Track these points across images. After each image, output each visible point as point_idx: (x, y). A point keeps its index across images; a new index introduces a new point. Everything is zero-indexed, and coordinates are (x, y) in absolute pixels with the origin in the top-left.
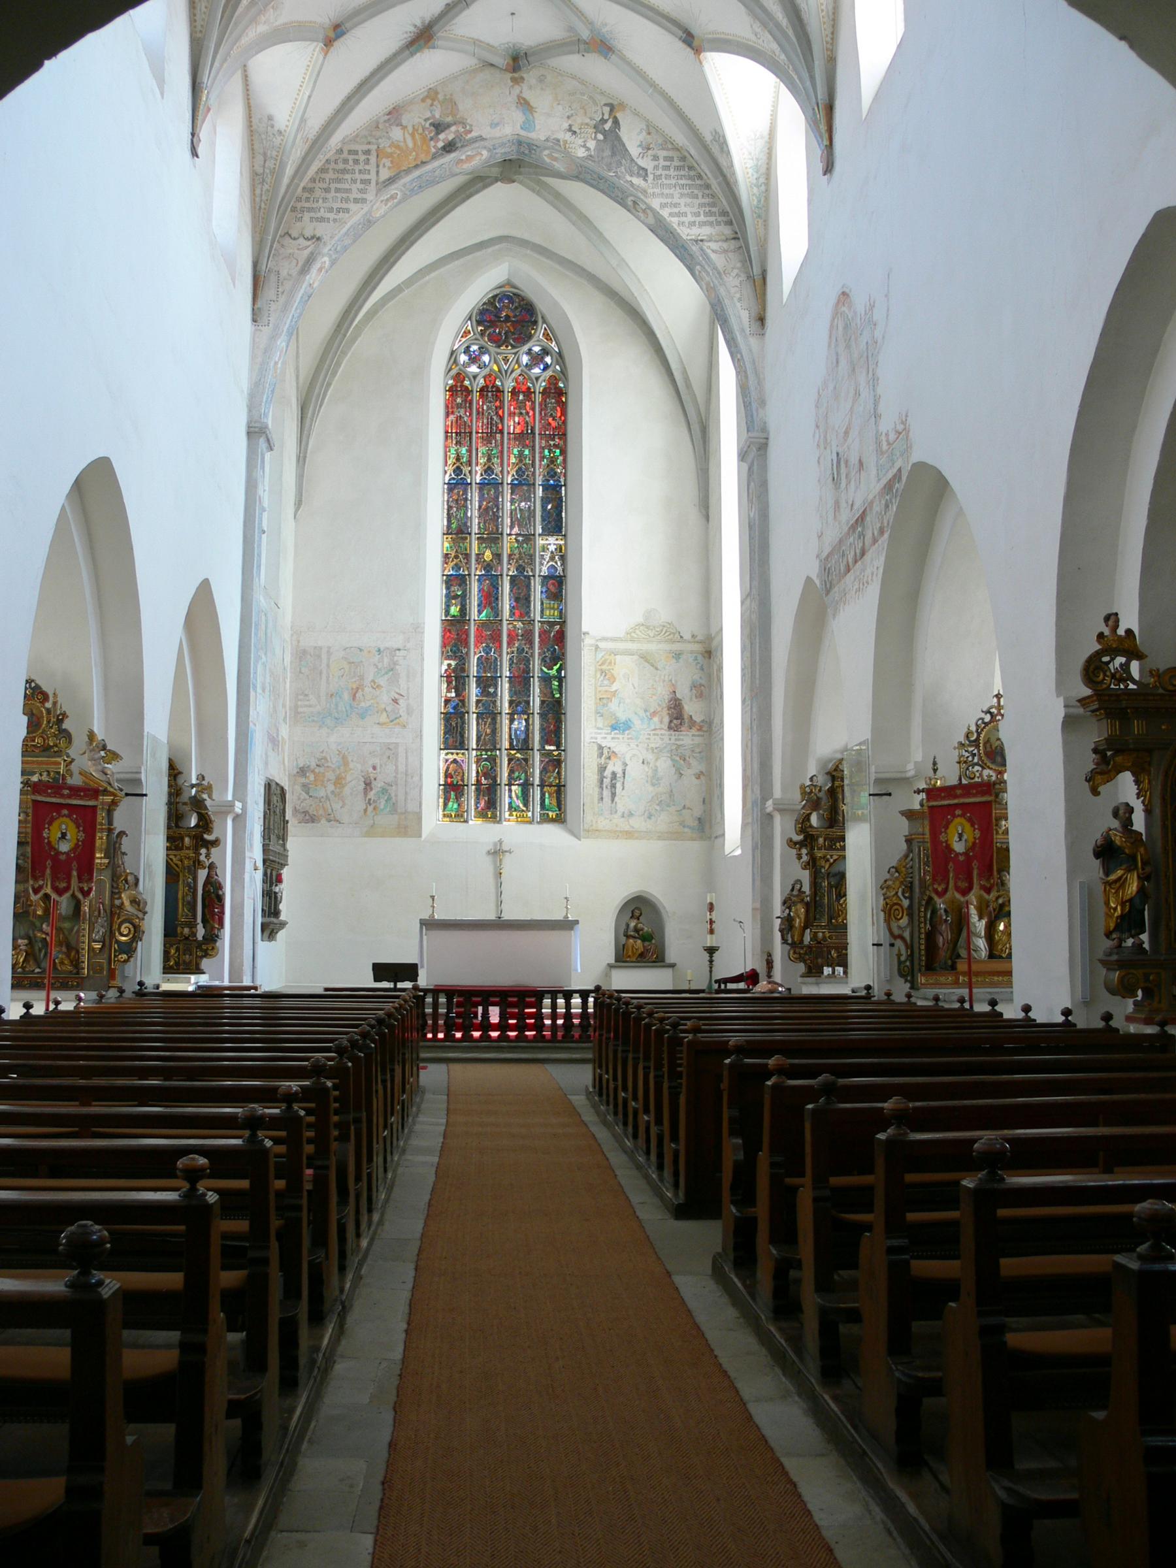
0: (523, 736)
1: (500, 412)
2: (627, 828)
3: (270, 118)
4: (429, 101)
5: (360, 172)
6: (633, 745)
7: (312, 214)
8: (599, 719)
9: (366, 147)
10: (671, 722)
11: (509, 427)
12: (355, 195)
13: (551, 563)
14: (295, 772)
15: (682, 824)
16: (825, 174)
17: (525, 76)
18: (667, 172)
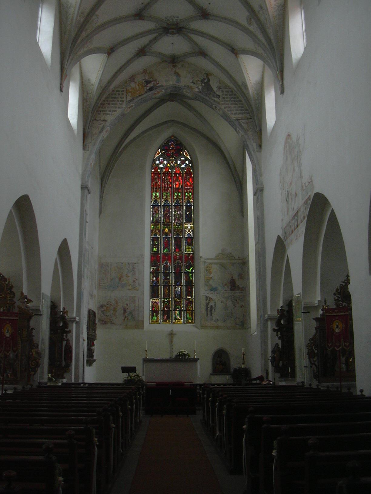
1: (171, 181)
3: (89, 80)
4: (144, 74)
5: (120, 98)
7: (104, 112)
8: (206, 287)
9: (122, 89)
10: (231, 288)
11: (174, 186)
12: (118, 106)
13: (189, 233)
14: (99, 306)
15: (236, 324)
16: (281, 94)
17: (177, 64)
18: (227, 96)
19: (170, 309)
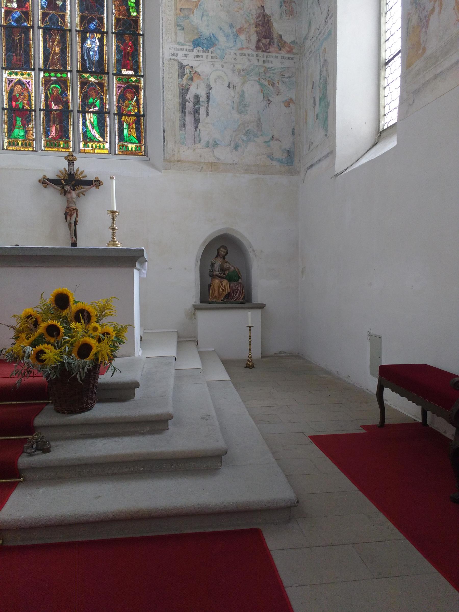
0: (97, 58)
2: (212, 159)
6: (218, 65)
8: (180, 33)
10: (259, 41)
15: (270, 156)
19: (68, 107)
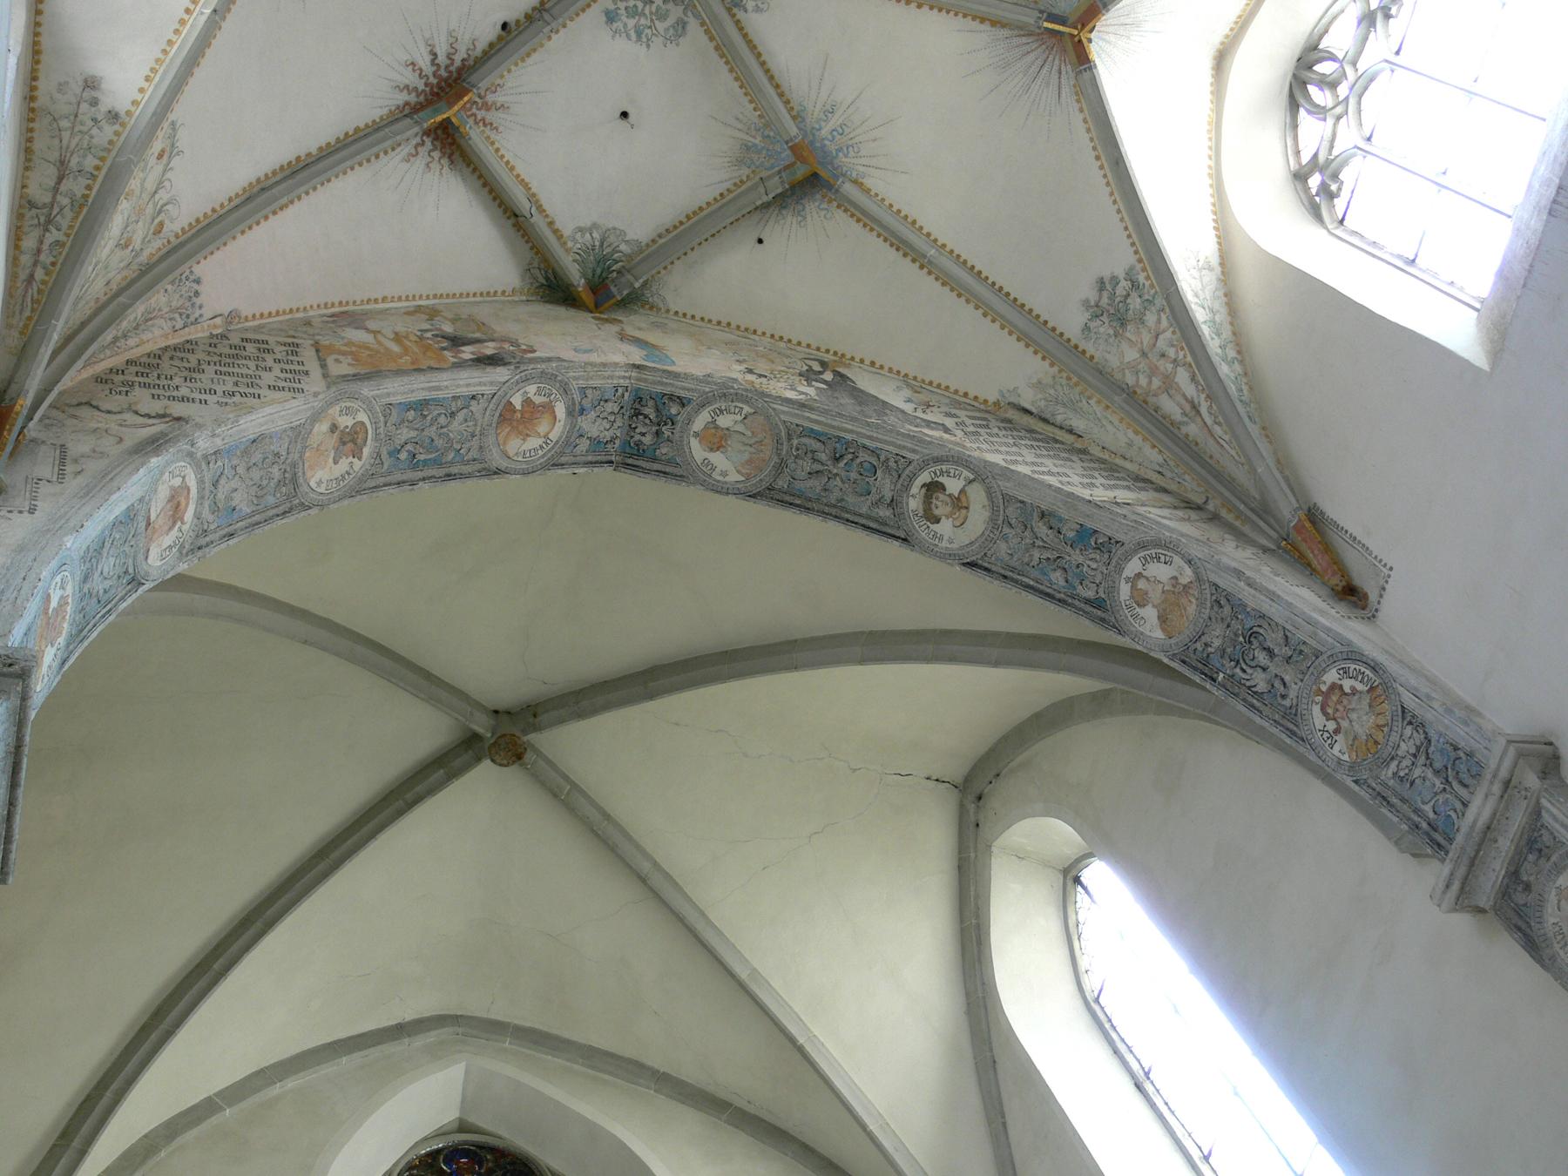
3: (91, 84)
